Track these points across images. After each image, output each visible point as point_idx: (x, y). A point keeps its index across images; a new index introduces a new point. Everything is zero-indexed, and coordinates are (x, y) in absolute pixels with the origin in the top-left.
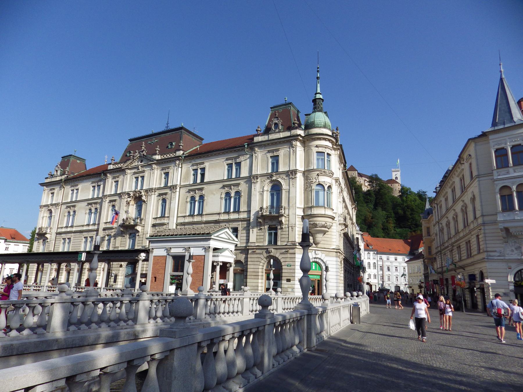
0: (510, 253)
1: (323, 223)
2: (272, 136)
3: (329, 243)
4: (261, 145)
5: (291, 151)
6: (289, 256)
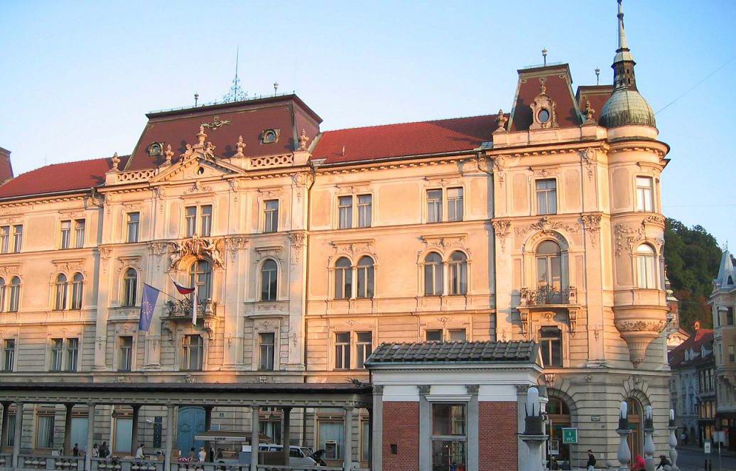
1: (657, 322)
2: (538, 137)
3: (654, 359)
4: (513, 151)
5: (585, 171)
6: (590, 389)
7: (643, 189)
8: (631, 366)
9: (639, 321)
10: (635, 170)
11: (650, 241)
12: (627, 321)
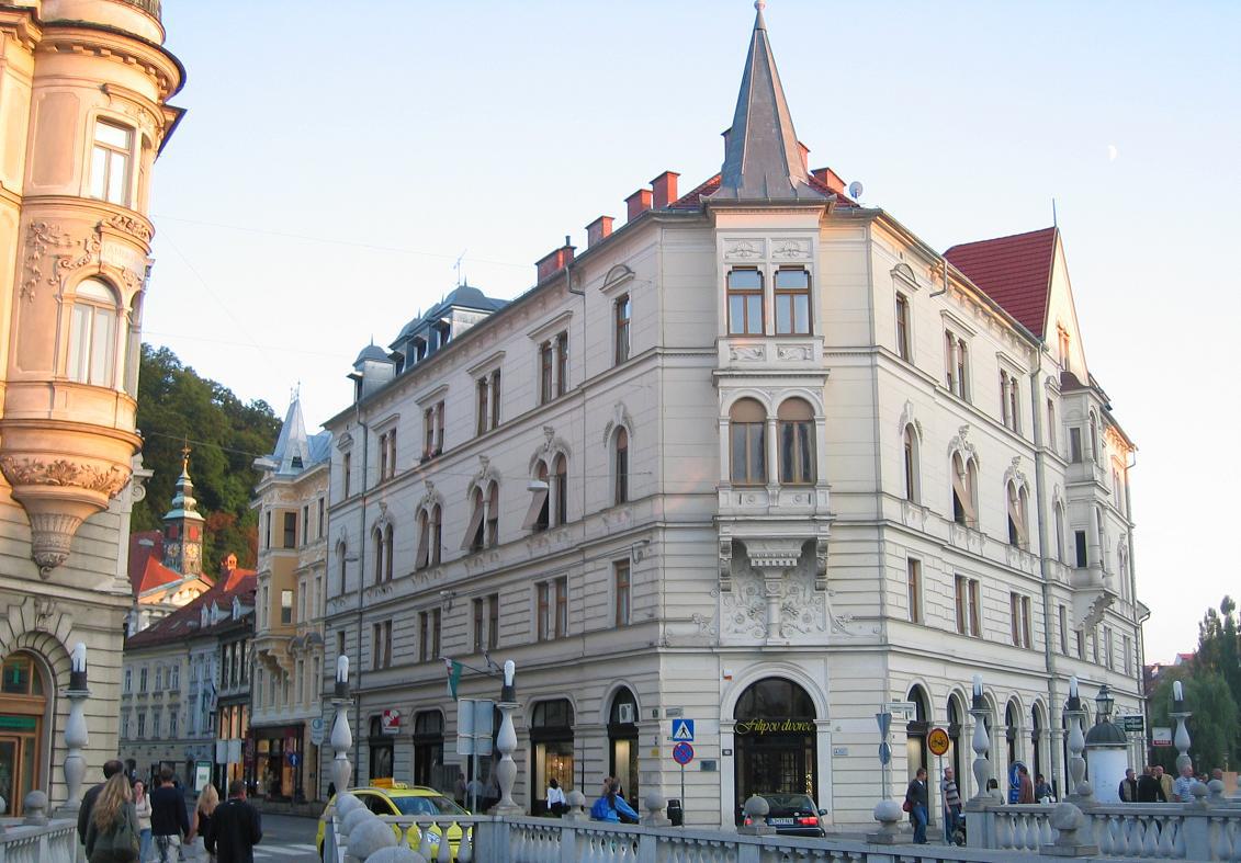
0: (735, 626)
1: (104, 468)
3: (91, 563)
7: (110, 150)
8: (34, 573)
9: (60, 459)
10: (95, 102)
11: (109, 274)
12: (31, 457)
